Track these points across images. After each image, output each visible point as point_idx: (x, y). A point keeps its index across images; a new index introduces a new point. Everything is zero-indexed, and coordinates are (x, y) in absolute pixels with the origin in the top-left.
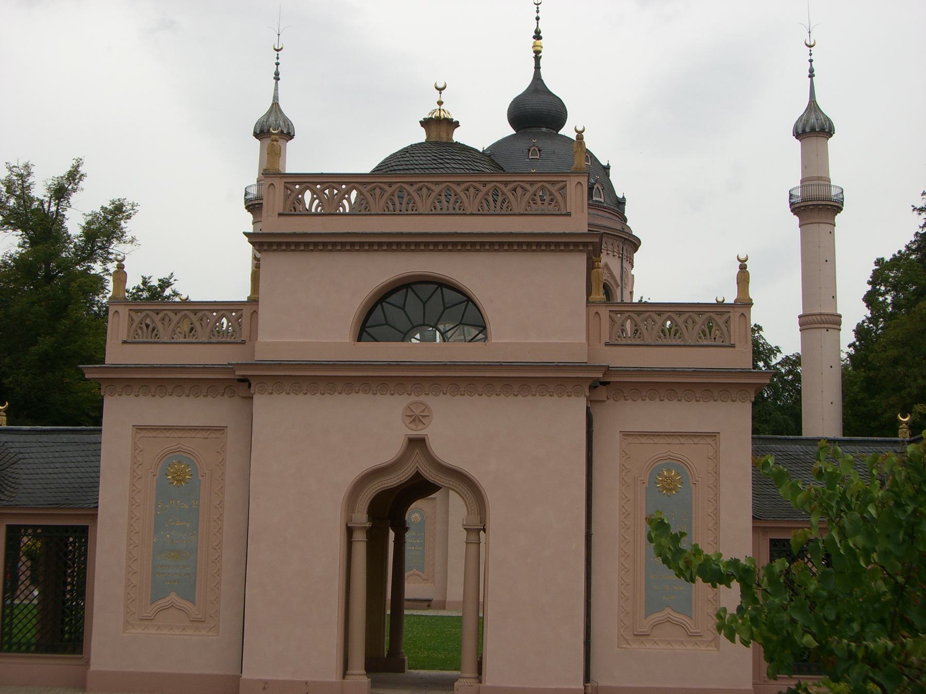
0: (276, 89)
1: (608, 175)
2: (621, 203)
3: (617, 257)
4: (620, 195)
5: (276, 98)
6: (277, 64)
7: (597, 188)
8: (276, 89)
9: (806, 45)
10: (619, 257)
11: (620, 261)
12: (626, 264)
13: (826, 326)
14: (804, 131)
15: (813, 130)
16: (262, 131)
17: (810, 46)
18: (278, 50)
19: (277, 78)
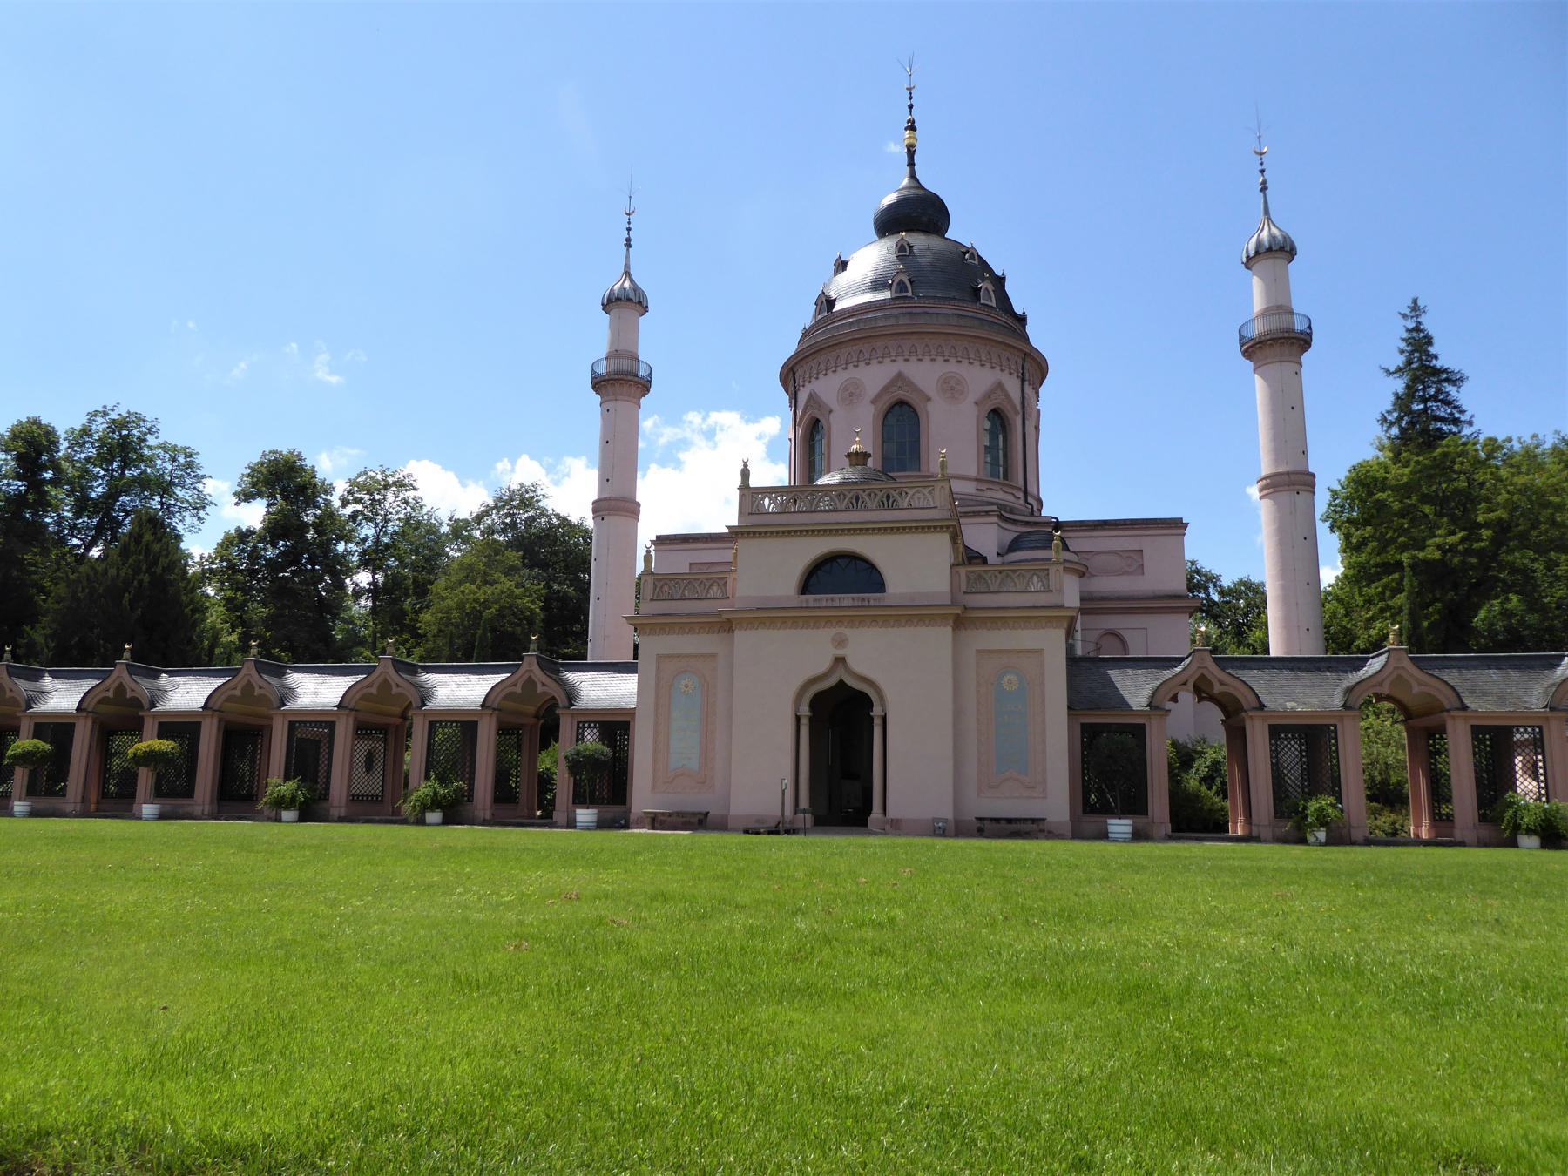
0: (628, 257)
1: (1003, 287)
2: (1022, 320)
3: (1015, 374)
4: (1018, 310)
5: (627, 266)
6: (629, 229)
7: (986, 289)
8: (628, 257)
9: (1256, 152)
10: (1018, 377)
11: (1018, 382)
12: (1028, 390)
13: (1298, 487)
14: (1257, 253)
15: (1270, 249)
16: (609, 300)
17: (1262, 154)
18: (629, 214)
19: (628, 244)
